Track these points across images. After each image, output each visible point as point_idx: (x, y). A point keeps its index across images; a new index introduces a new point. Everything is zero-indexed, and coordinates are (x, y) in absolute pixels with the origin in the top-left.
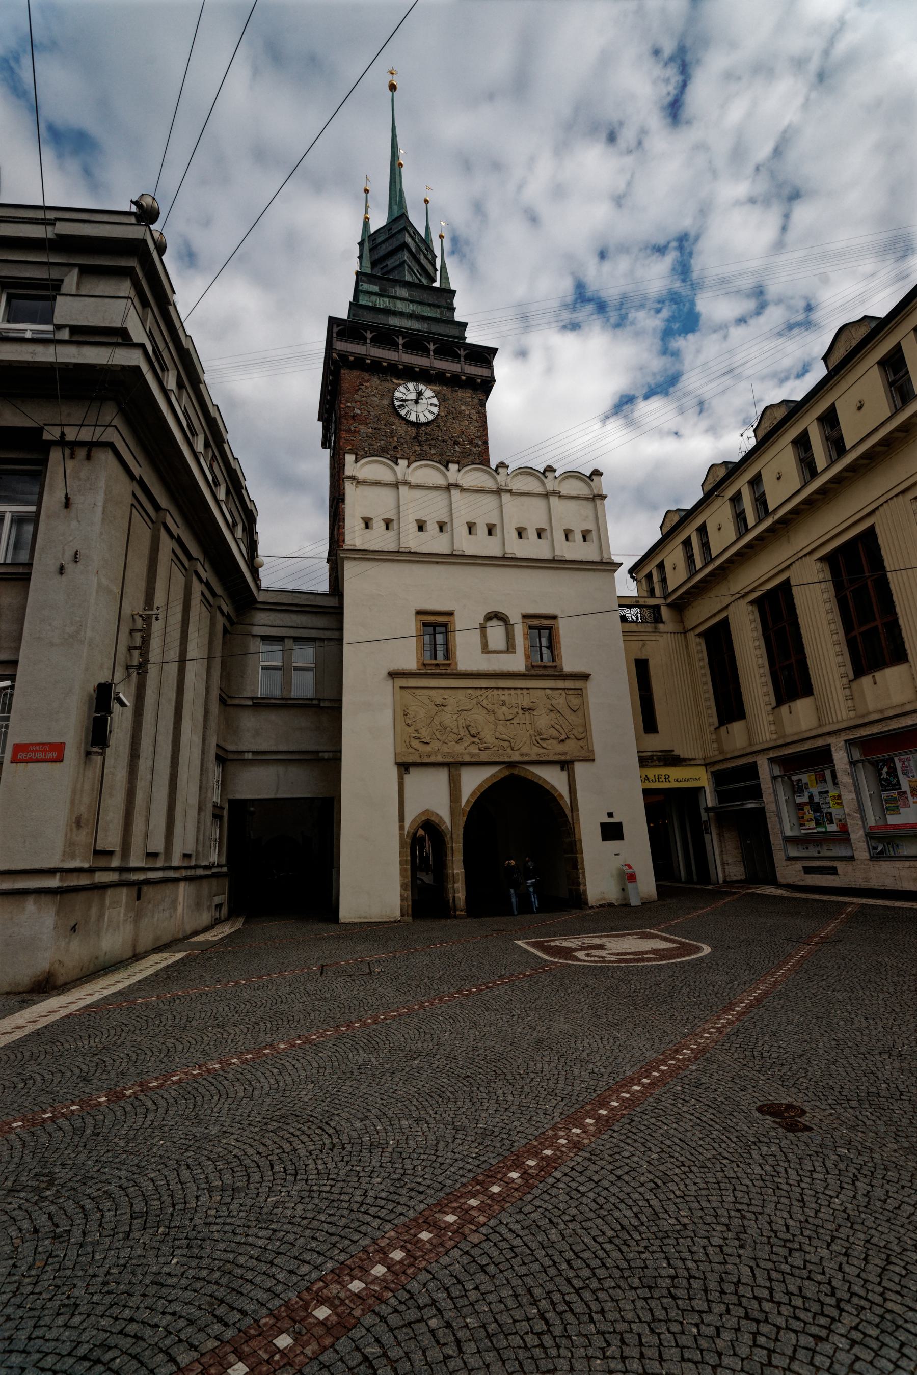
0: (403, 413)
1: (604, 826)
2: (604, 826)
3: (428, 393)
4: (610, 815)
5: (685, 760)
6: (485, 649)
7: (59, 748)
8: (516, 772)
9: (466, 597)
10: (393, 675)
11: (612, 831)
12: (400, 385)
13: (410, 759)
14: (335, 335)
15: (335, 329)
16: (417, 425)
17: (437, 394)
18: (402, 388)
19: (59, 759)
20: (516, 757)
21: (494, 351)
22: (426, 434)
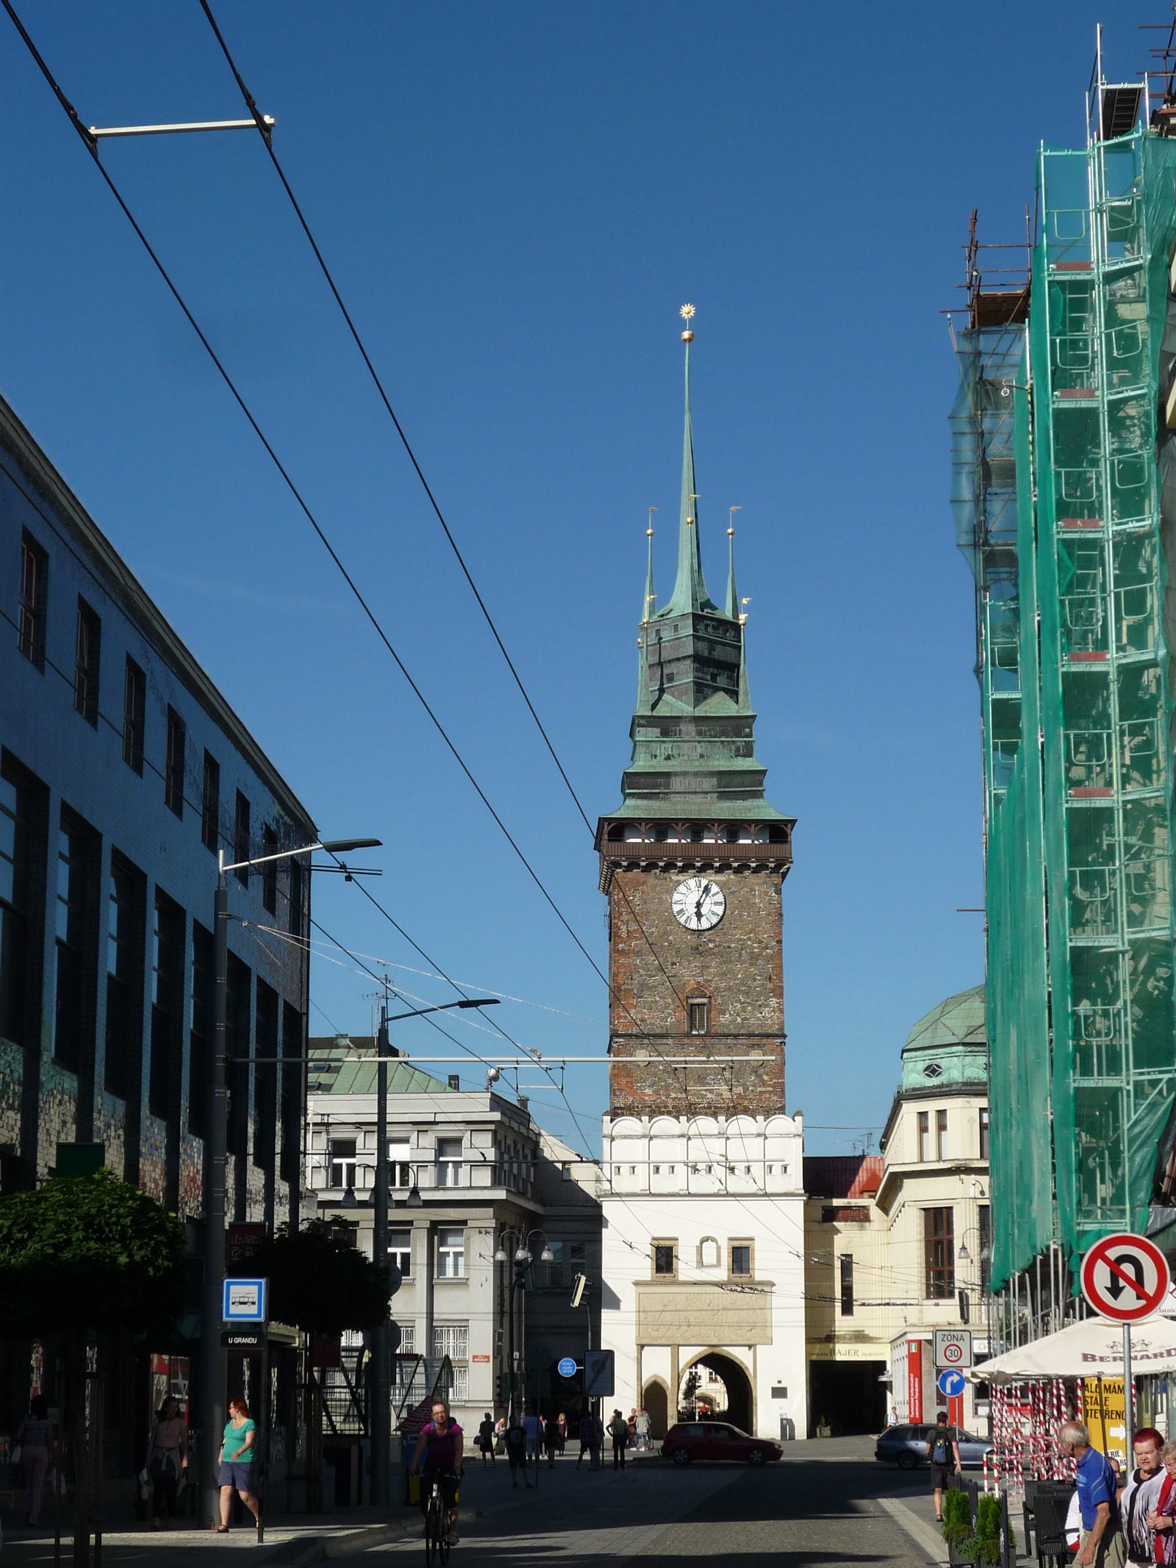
0: (682, 920)
1: (773, 1389)
2: (773, 1389)
3: (714, 889)
4: (779, 1382)
5: (872, 1338)
6: (701, 1264)
7: (488, 1357)
8: (716, 1350)
9: (685, 1225)
10: (636, 1284)
11: (779, 1392)
12: (679, 883)
13: (644, 1342)
14: (606, 837)
15: (606, 829)
16: (700, 932)
17: (722, 886)
18: (682, 888)
19: (474, 1357)
20: (715, 1342)
21: (793, 822)
22: (710, 941)
